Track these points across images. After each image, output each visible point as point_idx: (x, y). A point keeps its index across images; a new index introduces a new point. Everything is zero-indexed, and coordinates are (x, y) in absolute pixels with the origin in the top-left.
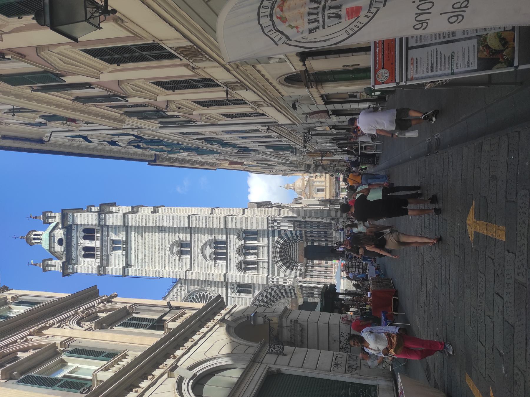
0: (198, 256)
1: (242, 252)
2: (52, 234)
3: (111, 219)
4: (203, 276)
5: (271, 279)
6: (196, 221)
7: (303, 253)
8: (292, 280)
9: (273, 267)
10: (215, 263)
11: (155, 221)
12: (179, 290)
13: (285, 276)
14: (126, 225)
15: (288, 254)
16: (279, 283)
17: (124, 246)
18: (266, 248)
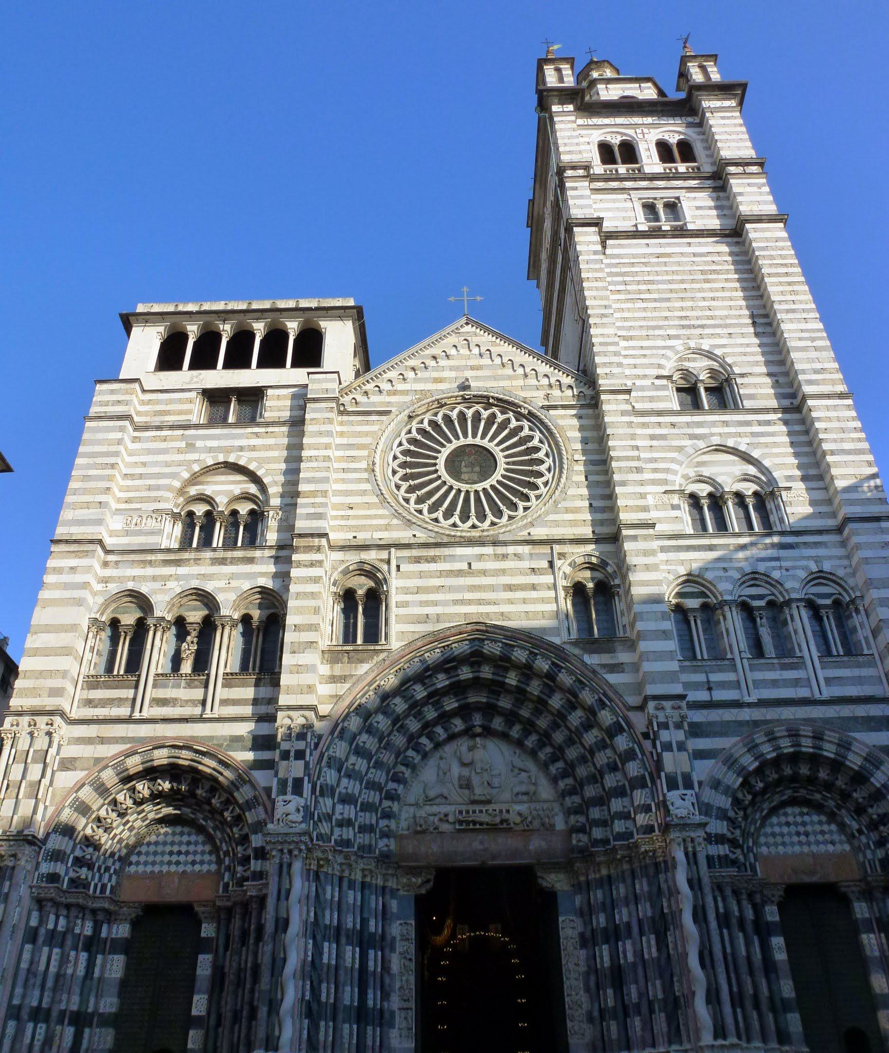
0: (693, 437)
1: (753, 597)
2: (649, 84)
3: (755, 189)
4: (624, 448)
5: (677, 719)
6: (838, 419)
7: (807, 879)
8: (698, 818)
9: (722, 729)
10: (681, 492)
11: (789, 298)
12: (545, 381)
13: (700, 783)
14: (748, 226)
15: (783, 804)
16: (667, 756)
17: (666, 228)
18: (803, 693)
